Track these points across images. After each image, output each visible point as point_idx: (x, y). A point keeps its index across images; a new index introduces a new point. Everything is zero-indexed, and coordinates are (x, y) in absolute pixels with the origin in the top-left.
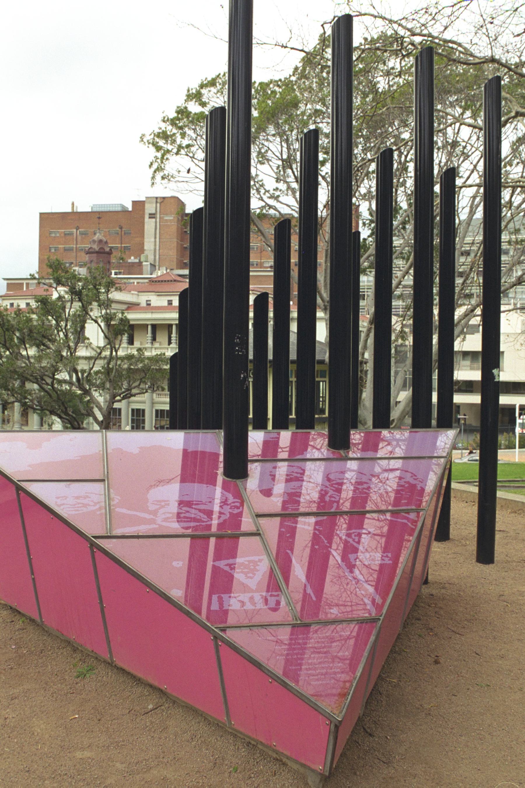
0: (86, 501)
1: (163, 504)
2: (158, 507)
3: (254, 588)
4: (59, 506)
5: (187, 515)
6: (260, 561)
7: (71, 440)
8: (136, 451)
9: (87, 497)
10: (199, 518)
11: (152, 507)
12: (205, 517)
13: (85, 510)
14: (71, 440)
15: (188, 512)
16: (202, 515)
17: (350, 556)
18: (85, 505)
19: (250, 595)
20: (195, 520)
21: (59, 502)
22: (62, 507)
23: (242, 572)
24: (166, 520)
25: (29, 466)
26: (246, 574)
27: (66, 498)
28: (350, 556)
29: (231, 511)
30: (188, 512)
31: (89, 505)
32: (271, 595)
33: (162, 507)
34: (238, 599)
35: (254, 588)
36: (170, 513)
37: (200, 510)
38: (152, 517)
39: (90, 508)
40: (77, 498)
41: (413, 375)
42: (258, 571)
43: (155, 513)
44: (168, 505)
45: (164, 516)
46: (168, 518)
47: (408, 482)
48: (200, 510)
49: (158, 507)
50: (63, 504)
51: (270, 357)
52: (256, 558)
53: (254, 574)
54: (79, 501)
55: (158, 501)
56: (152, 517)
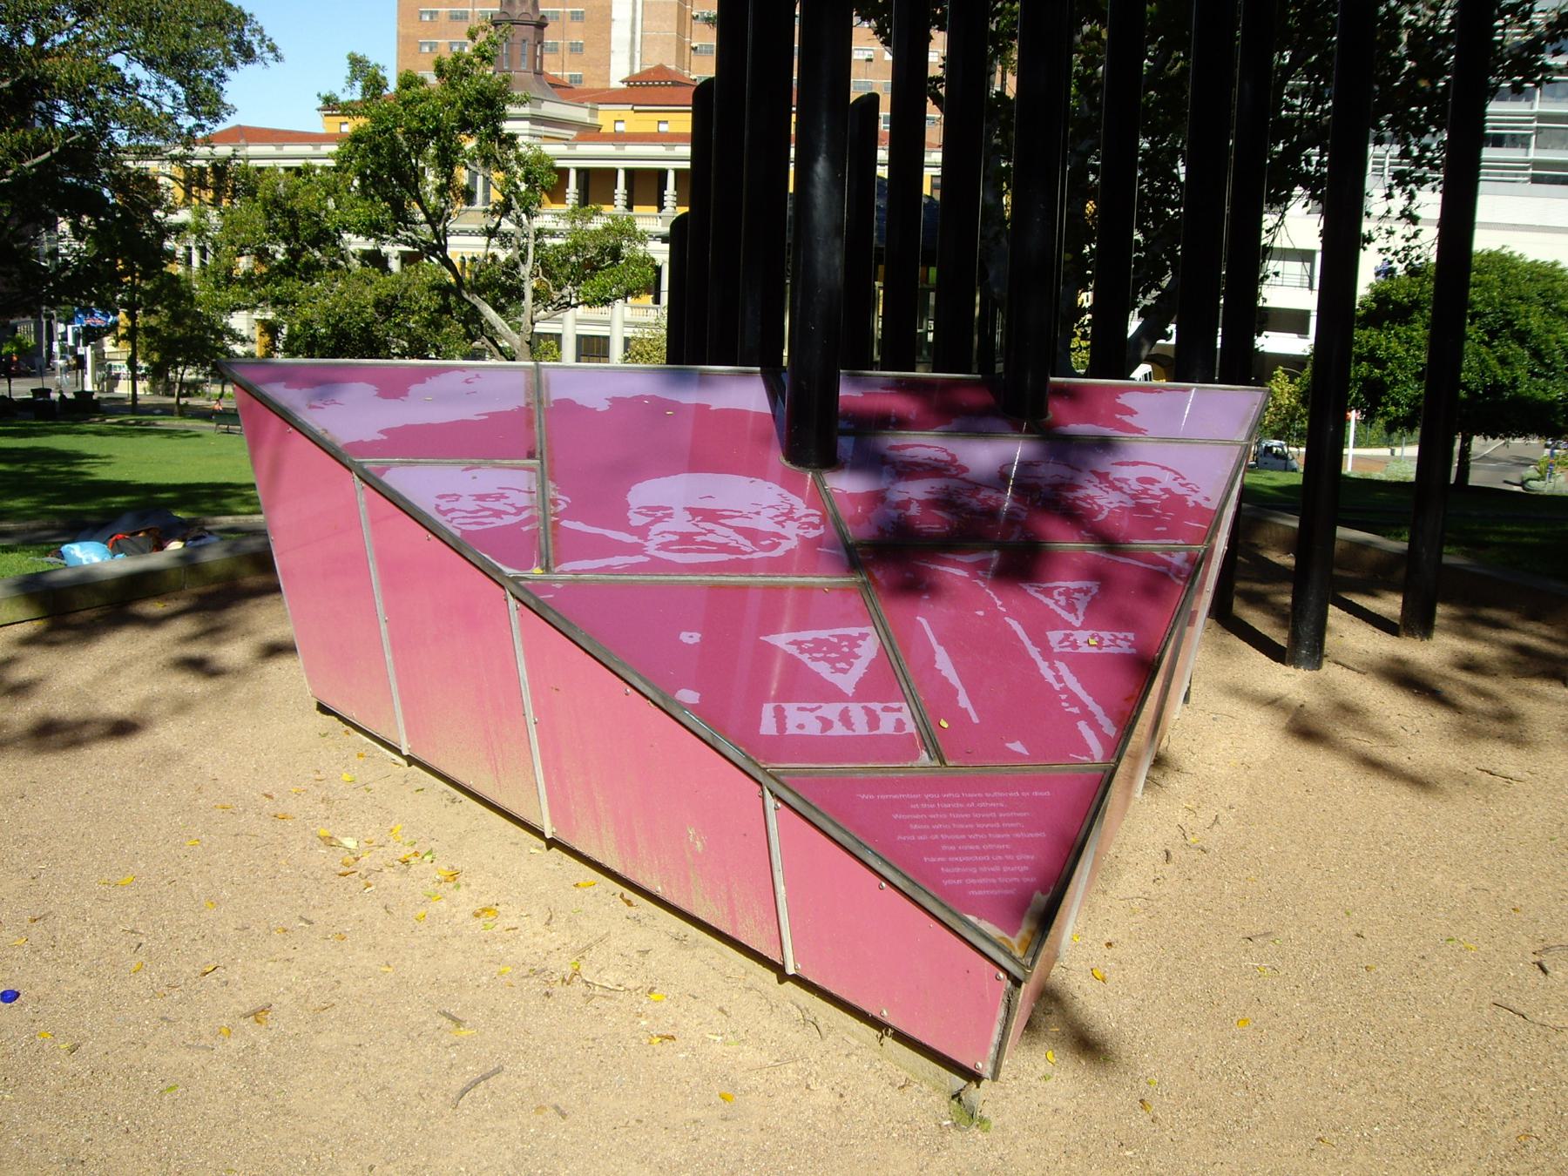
0: (499, 506)
1: (659, 514)
2: (648, 519)
3: (849, 690)
4: (444, 513)
5: (711, 538)
6: (863, 636)
7: (467, 381)
8: (603, 406)
9: (502, 496)
10: (733, 544)
11: (637, 520)
12: (748, 543)
13: (498, 522)
14: (467, 381)
15: (711, 531)
16: (741, 539)
17: (1049, 634)
18: (498, 514)
19: (844, 705)
20: (723, 548)
21: (445, 505)
22: (449, 516)
23: (825, 659)
24: (664, 547)
25: (381, 432)
26: (832, 662)
27: (457, 497)
28: (1049, 634)
29: (801, 532)
30: (711, 531)
31: (505, 513)
32: (886, 709)
33: (659, 520)
34: (819, 713)
35: (849, 690)
36: (675, 533)
37: (739, 530)
38: (634, 539)
39: (508, 520)
40: (481, 498)
41: (892, 123)
42: (857, 657)
43: (643, 532)
44: (670, 516)
45: (659, 540)
46: (671, 543)
47: (1166, 490)
48: (739, 530)
49: (648, 519)
50: (453, 510)
51: (791, 190)
52: (854, 631)
53: (851, 665)
54: (486, 504)
55: (649, 508)
56: (634, 539)
